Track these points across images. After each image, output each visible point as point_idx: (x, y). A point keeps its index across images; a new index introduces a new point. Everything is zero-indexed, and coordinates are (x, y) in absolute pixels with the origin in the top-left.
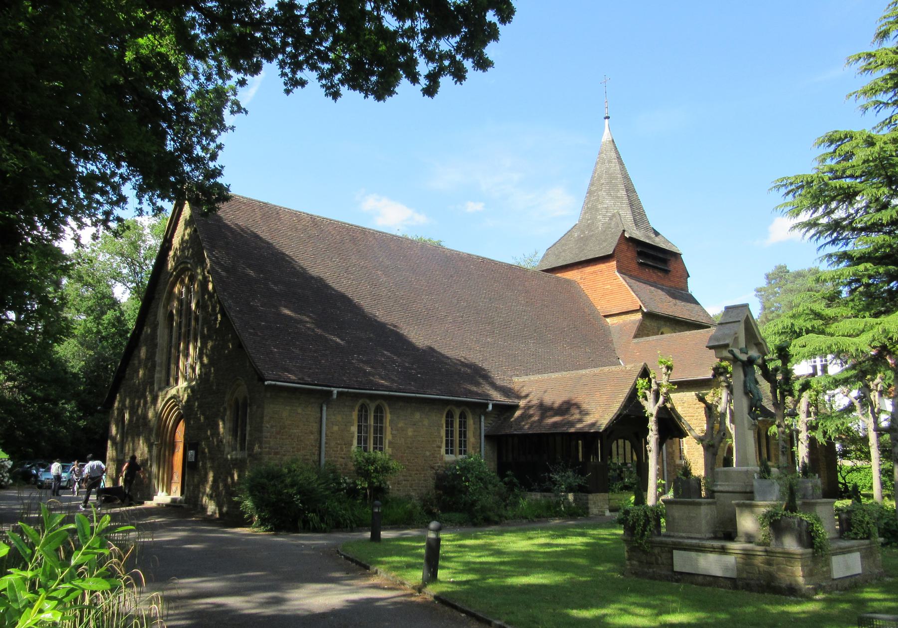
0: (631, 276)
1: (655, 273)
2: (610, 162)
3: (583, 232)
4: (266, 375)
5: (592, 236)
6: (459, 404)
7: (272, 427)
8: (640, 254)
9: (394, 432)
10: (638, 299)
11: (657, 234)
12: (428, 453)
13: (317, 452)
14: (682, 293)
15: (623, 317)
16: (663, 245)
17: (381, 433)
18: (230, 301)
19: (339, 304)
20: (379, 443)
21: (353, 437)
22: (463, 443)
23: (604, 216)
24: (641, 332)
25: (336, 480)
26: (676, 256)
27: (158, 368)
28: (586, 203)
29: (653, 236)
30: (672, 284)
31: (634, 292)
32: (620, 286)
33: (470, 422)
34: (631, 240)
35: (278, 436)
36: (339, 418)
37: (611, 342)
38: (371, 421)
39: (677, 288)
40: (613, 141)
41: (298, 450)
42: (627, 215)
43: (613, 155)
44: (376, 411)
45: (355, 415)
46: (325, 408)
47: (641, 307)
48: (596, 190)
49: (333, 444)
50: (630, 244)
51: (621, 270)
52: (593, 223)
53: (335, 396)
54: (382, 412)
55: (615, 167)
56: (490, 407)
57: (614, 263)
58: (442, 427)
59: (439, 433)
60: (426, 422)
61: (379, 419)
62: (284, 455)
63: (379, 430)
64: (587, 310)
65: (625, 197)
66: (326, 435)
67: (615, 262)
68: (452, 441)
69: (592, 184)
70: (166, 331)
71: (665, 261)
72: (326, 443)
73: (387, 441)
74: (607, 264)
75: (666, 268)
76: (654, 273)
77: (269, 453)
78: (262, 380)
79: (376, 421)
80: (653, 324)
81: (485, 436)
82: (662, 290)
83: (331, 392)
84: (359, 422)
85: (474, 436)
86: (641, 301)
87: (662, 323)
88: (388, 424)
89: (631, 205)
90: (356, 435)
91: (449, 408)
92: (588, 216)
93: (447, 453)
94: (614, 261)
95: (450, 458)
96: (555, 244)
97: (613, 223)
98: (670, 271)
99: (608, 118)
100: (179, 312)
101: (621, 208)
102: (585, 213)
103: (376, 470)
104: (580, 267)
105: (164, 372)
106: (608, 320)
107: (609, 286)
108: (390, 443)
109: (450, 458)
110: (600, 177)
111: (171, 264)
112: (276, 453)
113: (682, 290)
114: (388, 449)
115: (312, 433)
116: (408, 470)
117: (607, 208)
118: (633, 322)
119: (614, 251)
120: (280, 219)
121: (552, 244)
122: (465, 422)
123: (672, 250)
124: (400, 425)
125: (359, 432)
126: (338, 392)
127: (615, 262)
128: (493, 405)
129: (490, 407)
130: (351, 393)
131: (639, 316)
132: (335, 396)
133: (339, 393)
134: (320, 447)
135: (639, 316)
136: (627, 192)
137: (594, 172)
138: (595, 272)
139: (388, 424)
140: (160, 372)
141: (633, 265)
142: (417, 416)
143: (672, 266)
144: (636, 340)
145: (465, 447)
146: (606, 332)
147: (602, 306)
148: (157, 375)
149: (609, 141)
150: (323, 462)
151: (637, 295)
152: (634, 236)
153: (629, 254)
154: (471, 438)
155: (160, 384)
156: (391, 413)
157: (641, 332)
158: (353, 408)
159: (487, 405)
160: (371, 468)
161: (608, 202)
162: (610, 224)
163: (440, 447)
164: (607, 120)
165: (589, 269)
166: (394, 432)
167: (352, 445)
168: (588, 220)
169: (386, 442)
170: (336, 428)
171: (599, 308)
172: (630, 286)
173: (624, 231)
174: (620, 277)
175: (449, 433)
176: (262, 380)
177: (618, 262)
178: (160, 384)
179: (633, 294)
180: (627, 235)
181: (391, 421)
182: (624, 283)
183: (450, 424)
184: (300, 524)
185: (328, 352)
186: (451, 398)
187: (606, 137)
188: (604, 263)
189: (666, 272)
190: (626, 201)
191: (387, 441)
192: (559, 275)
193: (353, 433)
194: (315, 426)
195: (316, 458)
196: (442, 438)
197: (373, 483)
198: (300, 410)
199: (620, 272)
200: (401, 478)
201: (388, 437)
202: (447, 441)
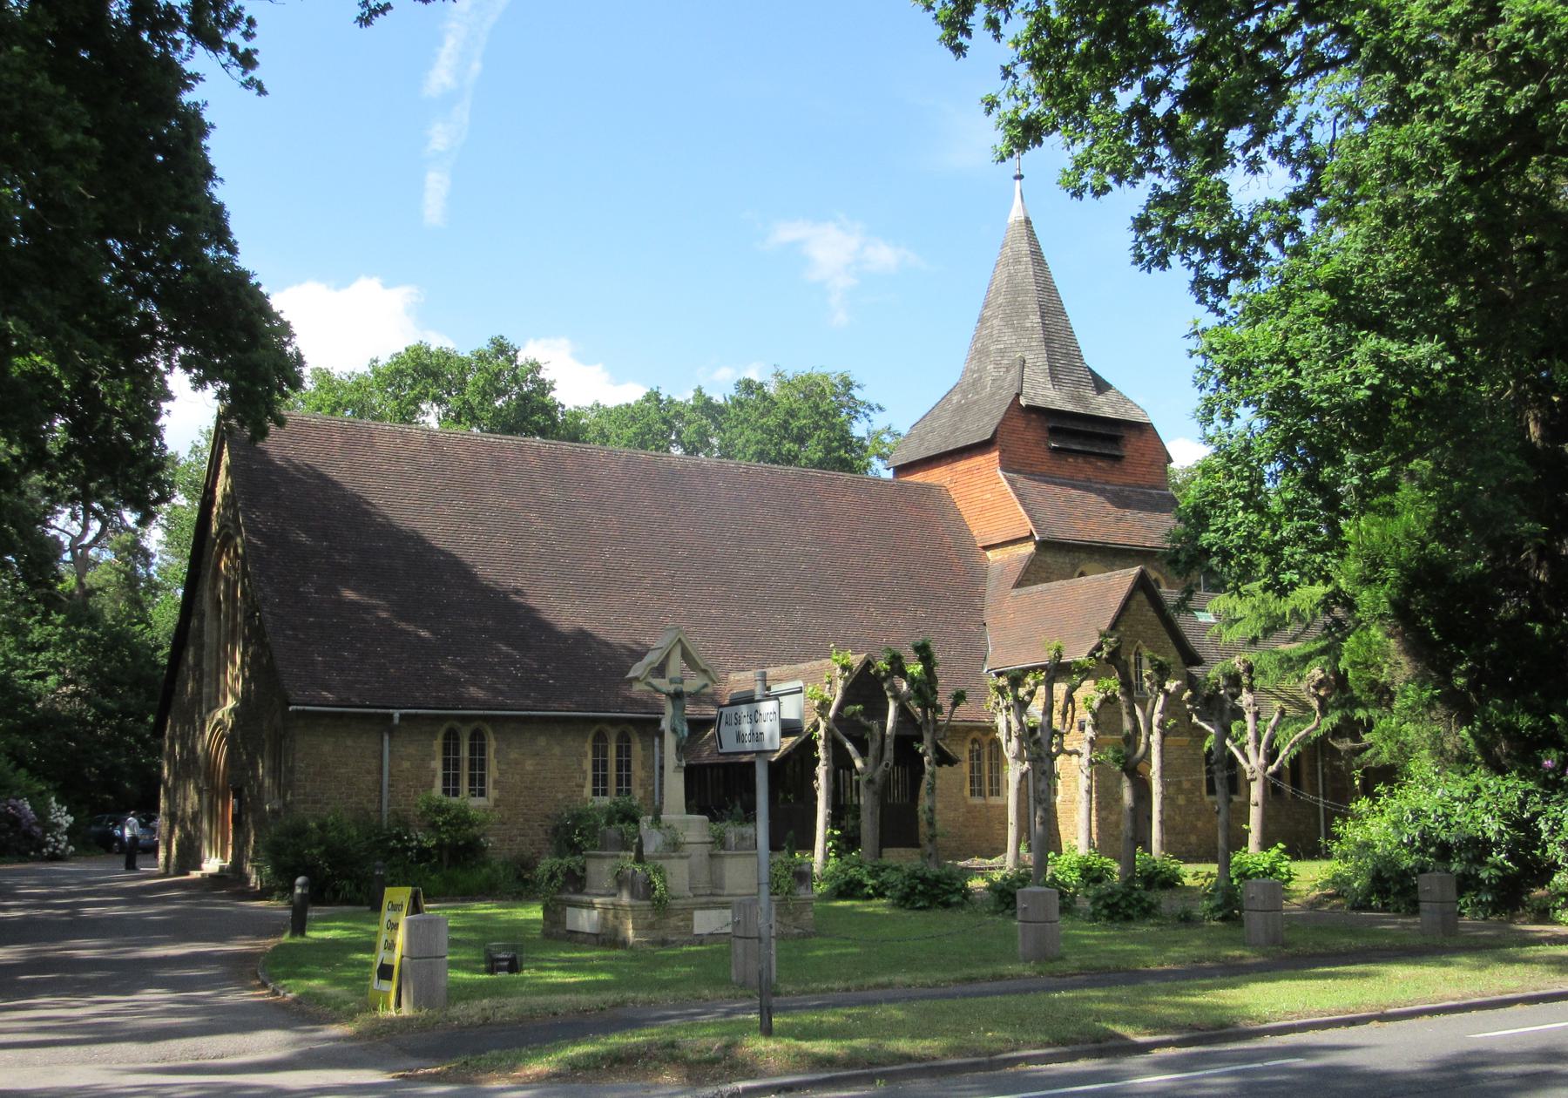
0: (1031, 475)
1: (1090, 463)
3: (964, 393)
5: (975, 402)
6: (614, 722)
8: (1055, 432)
9: (504, 767)
10: (1027, 519)
11: (1101, 386)
14: (1150, 494)
16: (1108, 412)
22: (624, 780)
23: (998, 365)
24: (1030, 575)
26: (1143, 429)
27: (206, 680)
28: (976, 339)
29: (1091, 393)
30: (1130, 480)
31: (1024, 505)
32: (1004, 495)
33: (637, 748)
34: (1032, 410)
36: (411, 750)
37: (982, 596)
38: (465, 753)
39: (1140, 486)
40: (1028, 221)
42: (1037, 361)
43: (1025, 248)
45: (438, 745)
46: (386, 738)
48: (991, 316)
51: (1006, 467)
52: (980, 377)
53: (396, 721)
54: (483, 738)
55: (1027, 268)
58: (586, 756)
59: (580, 765)
60: (557, 750)
61: (478, 749)
62: (327, 804)
64: (948, 540)
65: (1039, 328)
66: (391, 775)
67: (997, 453)
69: (986, 306)
71: (1115, 440)
72: (390, 786)
74: (987, 456)
75: (1117, 453)
80: (1061, 560)
82: (1101, 492)
83: (390, 716)
84: (444, 754)
86: (1034, 522)
87: (1083, 556)
89: (1048, 341)
90: (440, 773)
91: (597, 727)
92: (974, 366)
98: (1123, 457)
99: (1020, 177)
101: (1029, 348)
102: (972, 359)
106: (989, 554)
108: (495, 782)
110: (998, 292)
111: (215, 527)
112: (315, 802)
114: (492, 793)
115: (369, 772)
116: (527, 820)
120: (373, 446)
122: (628, 749)
123: (1127, 418)
126: (401, 715)
127: (997, 453)
130: (422, 715)
132: (396, 721)
133: (402, 717)
134: (381, 792)
136: (1042, 317)
137: (991, 284)
138: (969, 470)
142: (542, 741)
144: (1015, 592)
147: (983, 529)
149: (1020, 222)
152: (1039, 402)
153: (1030, 436)
156: (496, 739)
157: (1030, 575)
158: (433, 735)
160: (440, 820)
161: (1009, 338)
165: (962, 465)
166: (504, 767)
168: (974, 372)
169: (490, 781)
170: (406, 765)
171: (975, 533)
172: (1018, 496)
173: (1018, 395)
175: (599, 765)
179: (1021, 509)
180: (1023, 402)
181: (497, 752)
182: (1010, 490)
186: (591, 714)
187: (1016, 213)
188: (982, 453)
189: (1118, 459)
190: (1039, 335)
193: (434, 771)
196: (585, 772)
197: (442, 840)
198: (349, 742)
199: (1002, 469)
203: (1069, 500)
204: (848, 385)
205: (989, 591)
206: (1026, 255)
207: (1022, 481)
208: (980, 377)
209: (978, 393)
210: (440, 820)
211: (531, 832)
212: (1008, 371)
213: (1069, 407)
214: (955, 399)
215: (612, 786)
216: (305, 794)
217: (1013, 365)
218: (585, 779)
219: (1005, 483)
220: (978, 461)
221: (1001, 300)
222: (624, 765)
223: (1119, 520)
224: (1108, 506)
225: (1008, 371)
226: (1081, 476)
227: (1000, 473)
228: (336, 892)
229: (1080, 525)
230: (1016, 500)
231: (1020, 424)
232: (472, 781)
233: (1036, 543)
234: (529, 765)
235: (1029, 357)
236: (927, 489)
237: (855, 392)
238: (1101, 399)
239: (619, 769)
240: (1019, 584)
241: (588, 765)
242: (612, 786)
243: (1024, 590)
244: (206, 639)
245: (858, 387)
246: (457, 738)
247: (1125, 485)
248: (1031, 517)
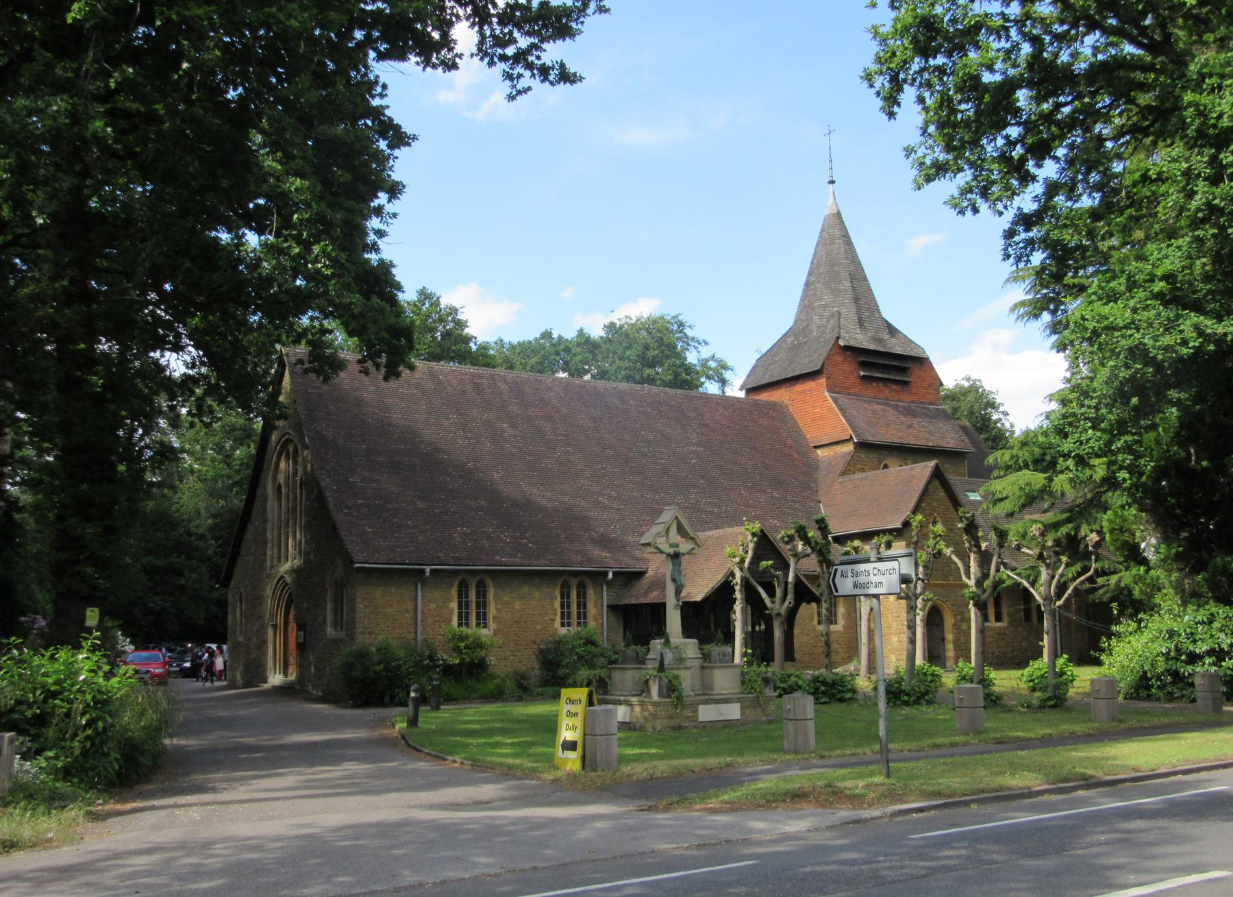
2: (832, 243)
3: (796, 337)
4: (355, 560)
5: (805, 343)
7: (365, 607)
8: (863, 365)
10: (848, 427)
11: (892, 330)
12: (539, 627)
13: (413, 631)
15: (835, 447)
16: (899, 350)
17: (485, 608)
18: (327, 480)
19: (450, 470)
20: (482, 619)
21: (452, 614)
22: (582, 616)
23: (821, 317)
24: (849, 468)
25: (431, 658)
26: (921, 362)
27: (269, 545)
29: (886, 337)
30: (915, 398)
31: (845, 416)
32: (830, 409)
33: (591, 593)
34: (847, 348)
35: (373, 616)
36: (436, 595)
37: (816, 482)
40: (839, 214)
41: (394, 629)
42: (849, 312)
43: (837, 233)
44: (478, 586)
45: (454, 592)
46: (419, 586)
47: (851, 437)
49: (430, 621)
52: (808, 325)
53: (428, 574)
54: (485, 586)
56: (610, 575)
57: (823, 381)
59: (552, 605)
61: (482, 594)
63: (482, 605)
64: (790, 441)
65: (850, 290)
66: (423, 613)
68: (569, 613)
70: (276, 505)
72: (422, 621)
73: (491, 616)
74: (817, 382)
76: (885, 386)
77: (363, 633)
78: (352, 562)
79: (478, 596)
81: (609, 606)
83: (423, 571)
85: (595, 607)
86: (853, 428)
87: (886, 453)
88: (492, 599)
89: (856, 299)
90: (456, 611)
91: (564, 578)
93: (563, 625)
95: (563, 631)
99: (832, 182)
100: (287, 484)
103: (466, 647)
105: (275, 549)
106: (819, 452)
108: (495, 618)
109: (563, 631)
112: (370, 633)
114: (492, 625)
116: (516, 645)
117: (824, 307)
119: (823, 364)
123: (912, 354)
124: (505, 599)
125: (460, 607)
126: (431, 570)
128: (614, 573)
129: (610, 575)
131: (849, 447)
132: (428, 574)
133: (431, 571)
134: (416, 625)
135: (849, 447)
136: (852, 282)
139: (492, 599)
140: (273, 547)
141: (853, 380)
142: (526, 589)
143: (914, 376)
145: (585, 618)
146: (811, 467)
147: (813, 433)
148: (269, 553)
149: (834, 214)
150: (420, 638)
151: (848, 421)
152: (853, 343)
153: (847, 367)
154: (592, 610)
155: (272, 561)
156: (494, 587)
157: (849, 468)
158: (452, 586)
159: (606, 573)
160: (462, 645)
161: (827, 298)
162: (826, 327)
163: (553, 620)
165: (799, 387)
167: (451, 621)
169: (490, 617)
170: (433, 605)
171: (808, 436)
173: (838, 338)
175: (565, 605)
176: (352, 562)
177: (828, 378)
178: (272, 561)
180: (841, 343)
181: (495, 596)
183: (565, 595)
184: (387, 699)
185: (428, 527)
189: (906, 383)
190: (850, 295)
191: (491, 616)
193: (453, 610)
194: (410, 606)
195: (412, 636)
196: (556, 610)
197: (464, 659)
199: (828, 391)
200: (508, 653)
201: (492, 611)
202: (562, 613)
203: (875, 413)
204: (681, 325)
205: (821, 478)
206: (839, 238)
208: (808, 325)
210: (462, 645)
211: (518, 654)
212: (829, 321)
213: (873, 347)
214: (789, 340)
215: (574, 620)
216: (364, 628)
217: (832, 316)
218: (556, 615)
219: (831, 401)
220: (810, 385)
221: (821, 270)
222: (582, 605)
223: (909, 427)
224: (901, 417)
225: (829, 321)
226: (882, 396)
227: (827, 394)
228: (392, 697)
230: (839, 413)
231: (839, 358)
232: (478, 617)
233: (854, 443)
234: (517, 605)
235: (843, 310)
236: (773, 406)
237: (688, 331)
238: (893, 341)
239: (579, 607)
241: (557, 604)
242: (574, 620)
243: (847, 478)
244: (269, 515)
245: (690, 327)
246: (467, 587)
247: (913, 402)
248: (851, 425)
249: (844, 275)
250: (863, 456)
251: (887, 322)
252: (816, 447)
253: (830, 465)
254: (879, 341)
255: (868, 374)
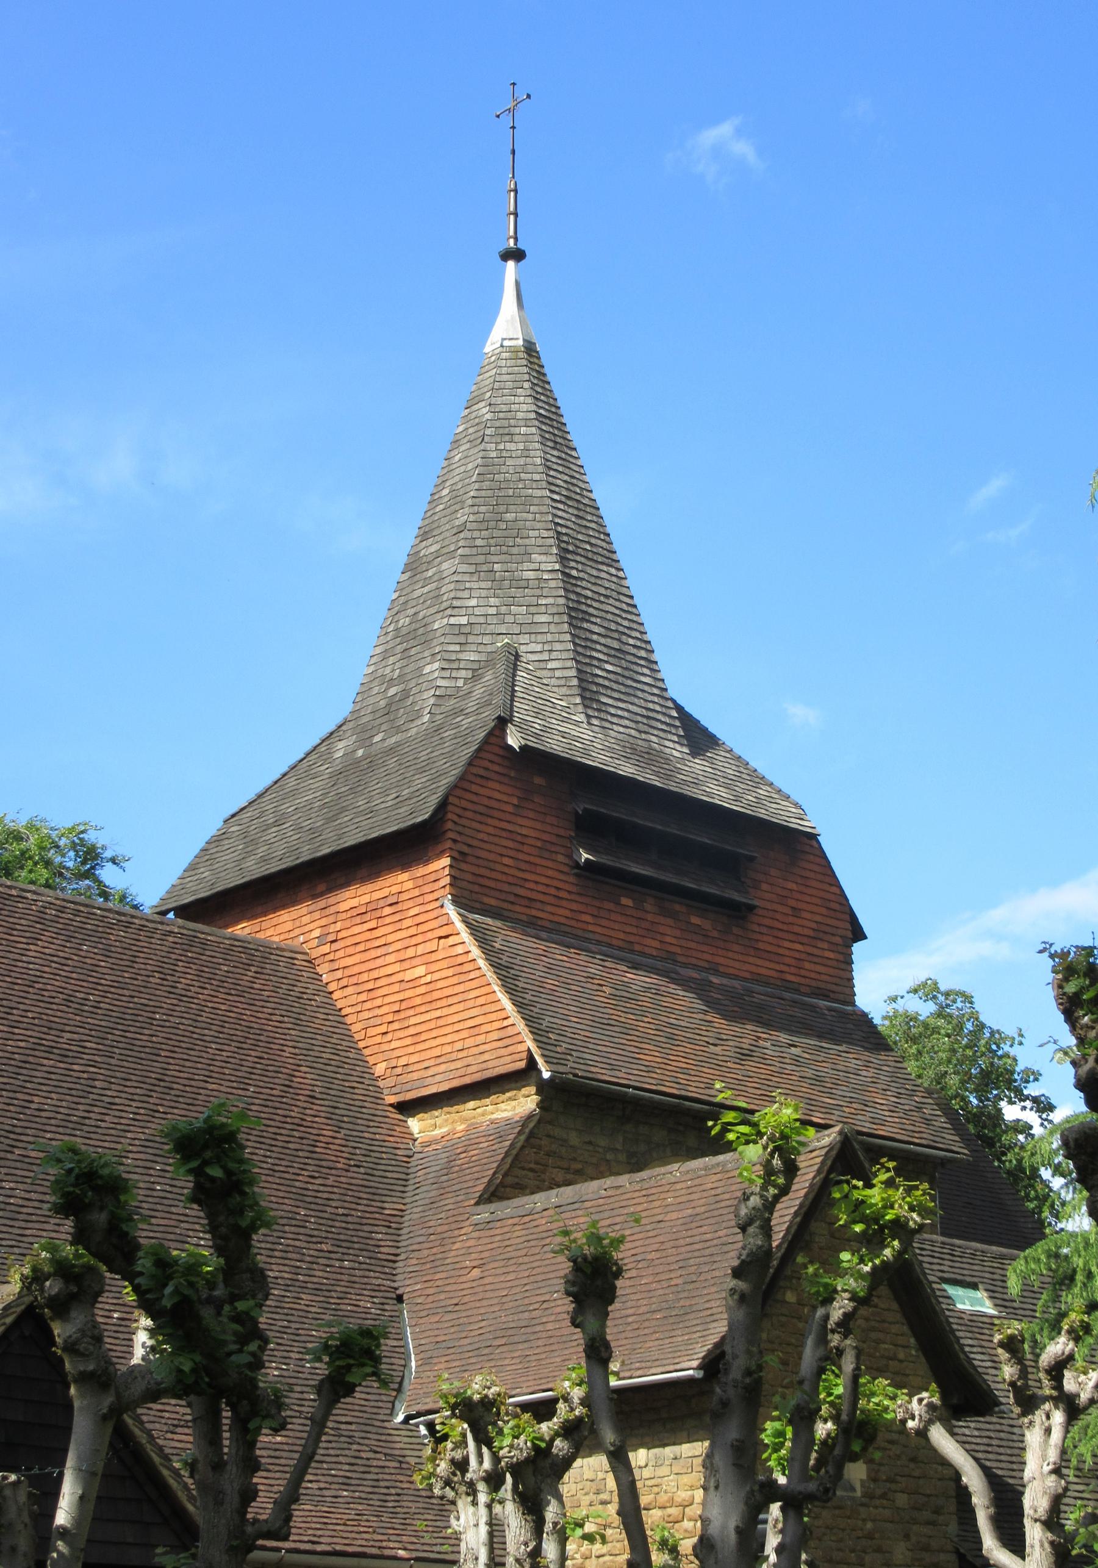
0: (531, 926)
3: (364, 735)
5: (391, 750)
10: (521, 1026)
14: (813, 1008)
16: (718, 795)
23: (450, 665)
28: (397, 609)
29: (677, 751)
31: (511, 991)
32: (461, 966)
37: (393, 1225)
39: (788, 987)
40: (530, 349)
43: (524, 406)
48: (437, 555)
50: (538, 780)
52: (406, 694)
64: (307, 1078)
65: (555, 584)
67: (446, 861)
69: (424, 535)
74: (421, 871)
75: (736, 896)
80: (603, 1142)
86: (537, 1033)
94: (439, 856)
96: (260, 796)
97: (478, 691)
98: (751, 908)
99: (516, 255)
101: (530, 629)
102: (385, 655)
104: (322, 887)
106: (415, 1124)
107: (420, 971)
110: (457, 499)
113: (825, 995)
118: (498, 1130)
119: (442, 806)
121: (251, 796)
127: (446, 861)
136: (563, 560)
138: (370, 910)
144: (484, 1214)
149: (514, 350)
151: (519, 1005)
152: (554, 745)
164: (511, 264)
171: (380, 1069)
172: (497, 967)
173: (502, 722)
174: (460, 926)
179: (506, 1002)
180: (513, 740)
182: (476, 952)
190: (554, 598)
192: (242, 929)
199: (456, 902)
203: (623, 996)
204: (91, 855)
205: (413, 1214)
206: (527, 423)
207: (505, 936)
208: (406, 694)
209: (398, 730)
212: (476, 676)
213: (627, 769)
214: (340, 749)
217: (489, 663)
219: (465, 935)
221: (461, 518)
223: (745, 1055)
224: (719, 1022)
225: (476, 676)
226: (652, 944)
229: (652, 1056)
230: (490, 975)
233: (543, 1087)
235: (529, 648)
237: (108, 875)
238: (698, 765)
240: (494, 1194)
245: (113, 861)
247: (758, 979)
248: (530, 1021)
249: (539, 535)
250: (574, 1139)
251: (679, 708)
252: (409, 1108)
253: (448, 1167)
254: (649, 757)
255: (606, 860)
